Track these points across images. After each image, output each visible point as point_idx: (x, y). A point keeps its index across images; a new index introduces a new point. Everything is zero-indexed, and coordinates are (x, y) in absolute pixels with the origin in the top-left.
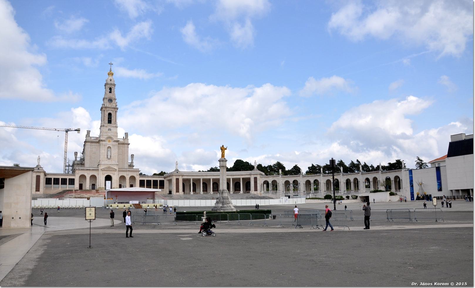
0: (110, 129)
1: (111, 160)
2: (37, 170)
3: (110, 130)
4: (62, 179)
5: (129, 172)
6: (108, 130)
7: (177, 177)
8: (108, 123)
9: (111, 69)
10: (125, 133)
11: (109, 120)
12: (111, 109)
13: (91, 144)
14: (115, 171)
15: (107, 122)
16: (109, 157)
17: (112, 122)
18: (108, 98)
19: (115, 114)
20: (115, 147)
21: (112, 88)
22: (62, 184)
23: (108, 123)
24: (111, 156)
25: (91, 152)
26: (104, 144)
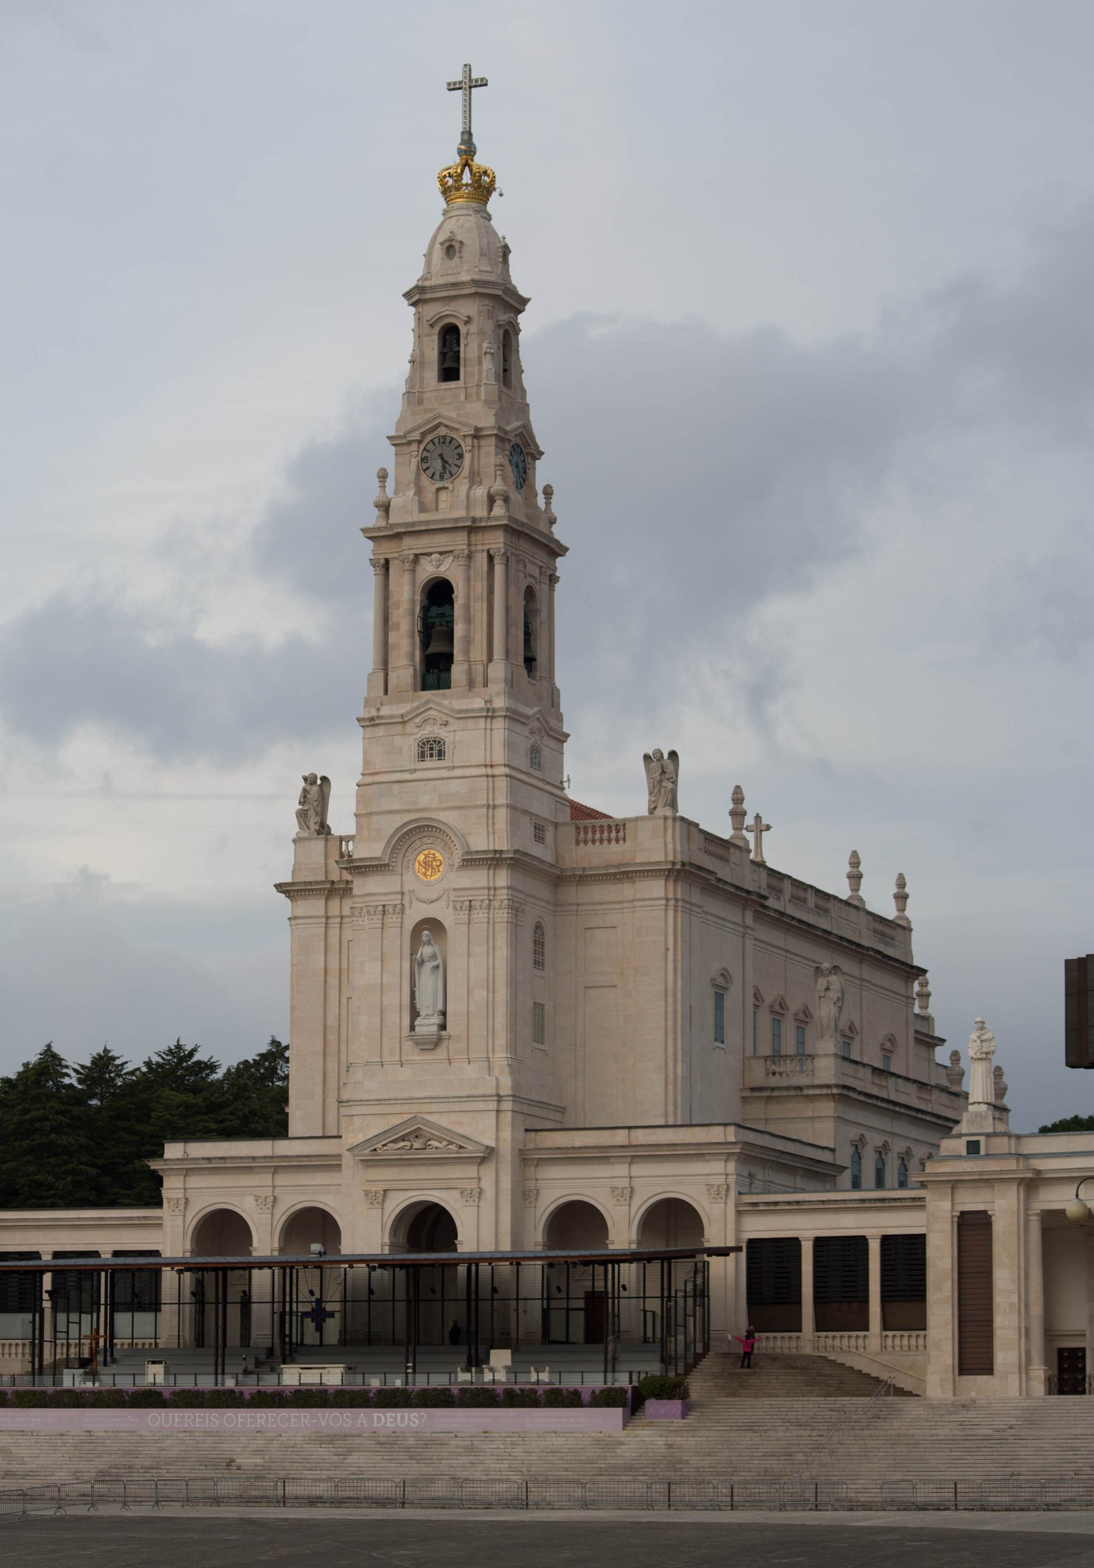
0: (438, 742)
1: (441, 1053)
3: (432, 749)
5: (633, 1159)
6: (415, 751)
7: (972, 1201)
9: (467, 137)
10: (647, 758)
11: (433, 649)
12: (442, 541)
13: (335, 903)
14: (483, 1160)
16: (427, 1025)
17: (458, 671)
18: (416, 436)
19: (479, 587)
20: (480, 916)
21: (463, 330)
24: (444, 1014)
25: (333, 981)
26: (380, 901)
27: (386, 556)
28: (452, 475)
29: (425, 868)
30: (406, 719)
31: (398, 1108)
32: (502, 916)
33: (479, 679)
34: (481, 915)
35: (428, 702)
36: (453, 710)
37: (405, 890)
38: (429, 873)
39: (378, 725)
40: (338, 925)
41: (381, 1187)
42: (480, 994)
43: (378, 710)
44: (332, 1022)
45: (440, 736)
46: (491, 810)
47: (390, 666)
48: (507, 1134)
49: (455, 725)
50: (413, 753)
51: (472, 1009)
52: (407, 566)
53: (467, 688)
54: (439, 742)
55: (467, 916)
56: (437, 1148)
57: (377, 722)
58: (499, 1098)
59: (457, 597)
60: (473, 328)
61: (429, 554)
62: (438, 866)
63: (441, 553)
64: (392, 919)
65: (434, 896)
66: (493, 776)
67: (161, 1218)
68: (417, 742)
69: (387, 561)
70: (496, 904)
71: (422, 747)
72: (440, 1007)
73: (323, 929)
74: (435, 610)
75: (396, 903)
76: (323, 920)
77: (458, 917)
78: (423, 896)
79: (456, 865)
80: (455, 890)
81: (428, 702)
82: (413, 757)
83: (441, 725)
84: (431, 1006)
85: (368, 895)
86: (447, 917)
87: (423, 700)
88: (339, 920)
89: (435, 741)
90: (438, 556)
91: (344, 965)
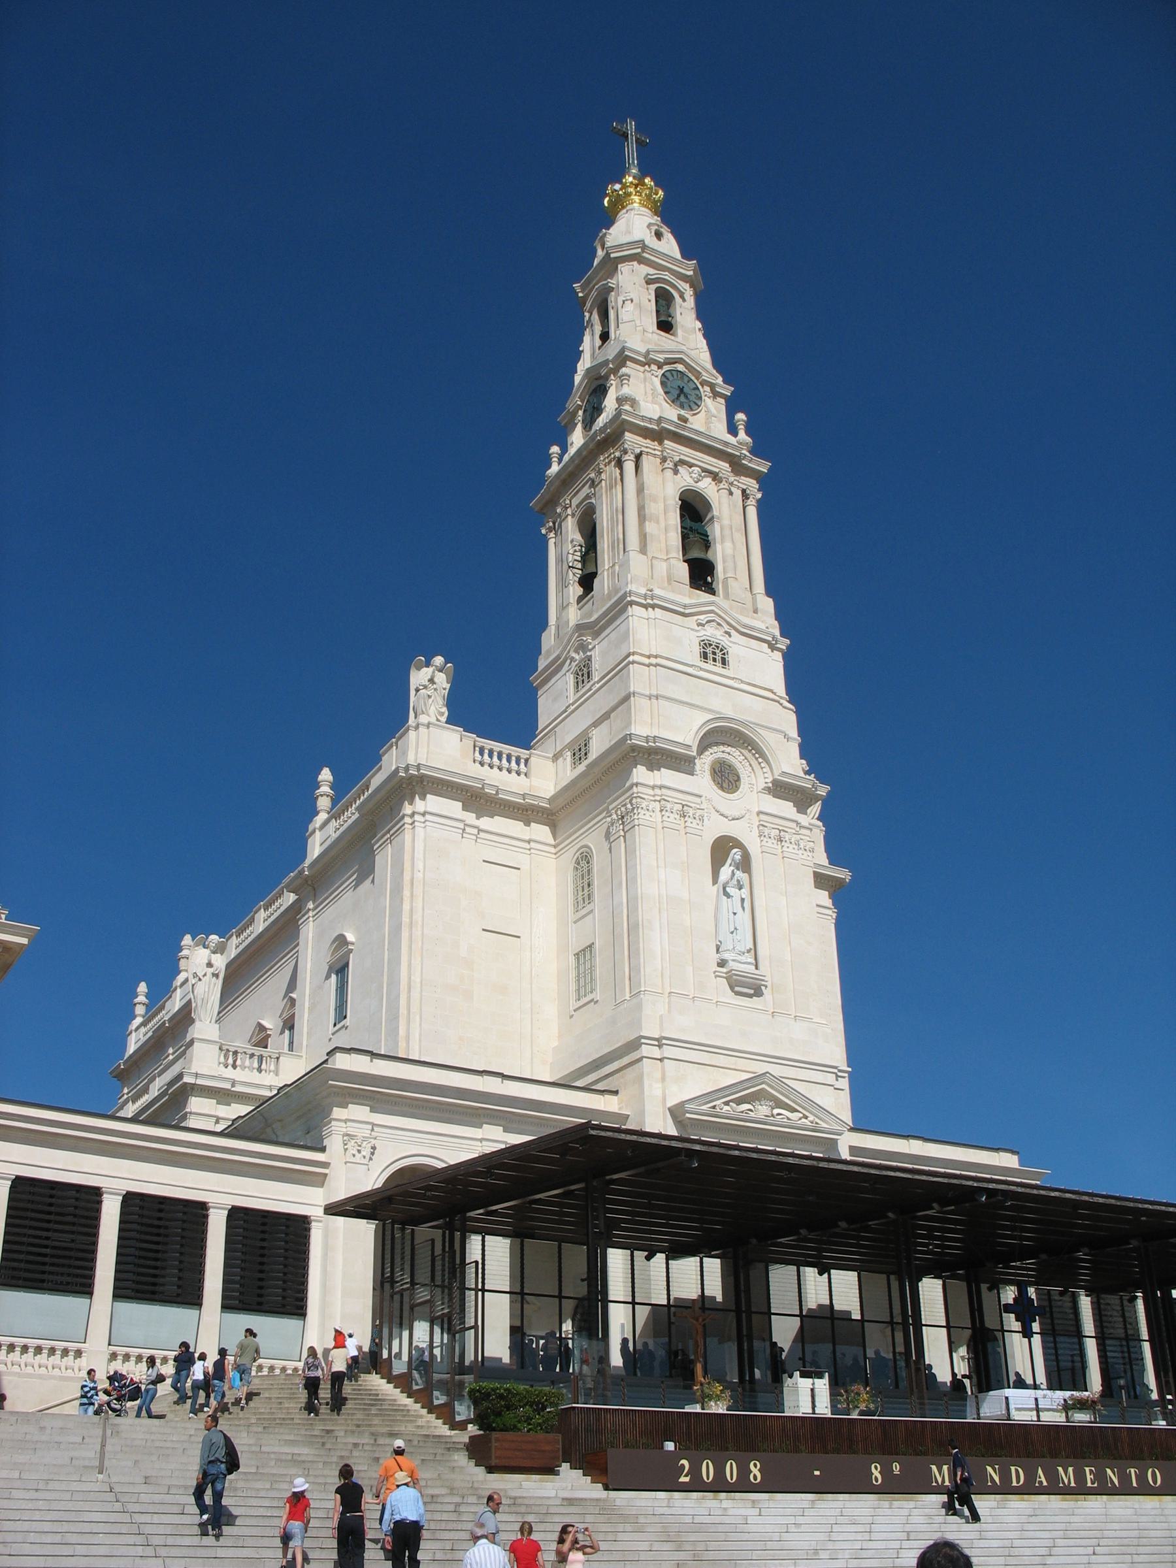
4: (132, 1201)
6: (697, 650)
11: (696, 554)
18: (661, 358)
27: (643, 449)
28: (692, 410)
30: (687, 611)
31: (721, 1060)
36: (738, 622)
38: (724, 785)
39: (653, 606)
45: (722, 643)
54: (722, 650)
56: (788, 1119)
57: (656, 601)
60: (685, 304)
61: (691, 465)
63: (704, 470)
65: (737, 814)
67: (325, 1165)
69: (641, 454)
71: (703, 648)
78: (722, 810)
80: (759, 813)
85: (661, 787)
90: (700, 470)
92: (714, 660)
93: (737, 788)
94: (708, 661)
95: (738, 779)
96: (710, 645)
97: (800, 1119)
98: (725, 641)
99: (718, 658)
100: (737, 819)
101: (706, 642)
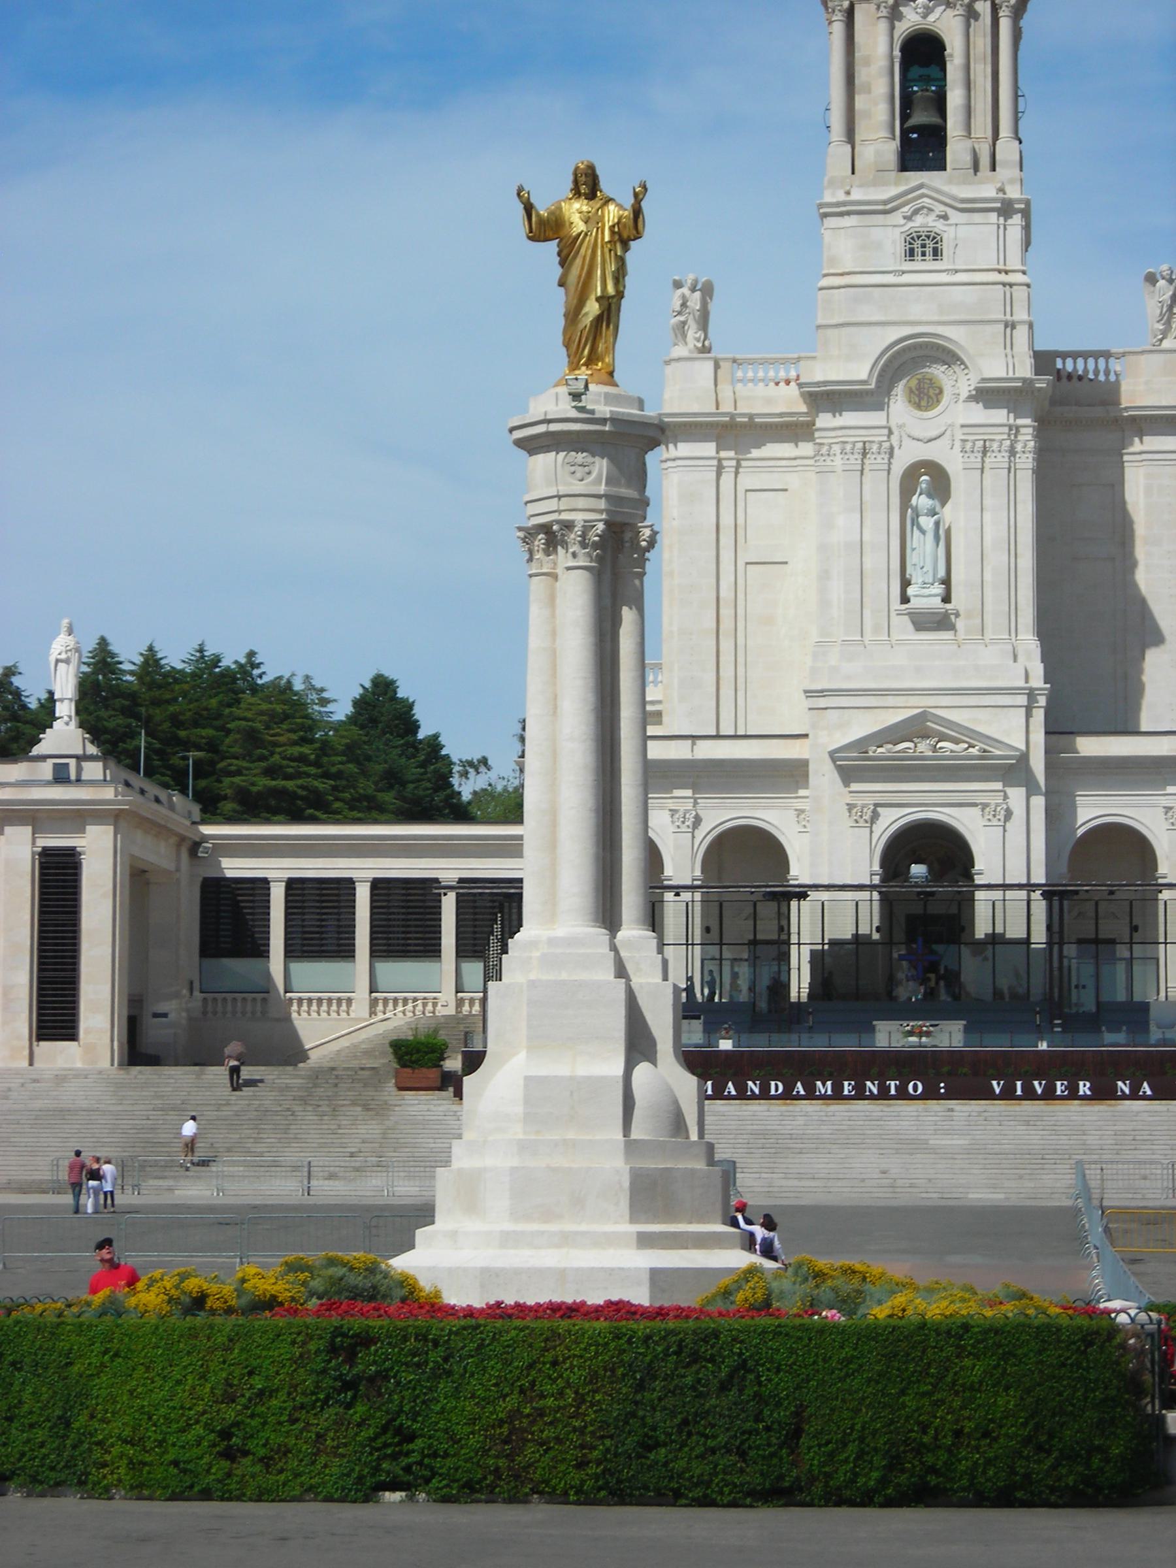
2: (48, 783)
6: (900, 248)
8: (905, 164)
11: (919, 118)
15: (890, 149)
16: (926, 597)
17: (956, 149)
19: (981, 43)
22: (383, 948)
23: (905, 164)
24: (947, 582)
29: (919, 396)
30: (889, 207)
31: (890, 701)
32: (1026, 462)
33: (985, 161)
34: (999, 459)
35: (921, 186)
36: (954, 198)
37: (893, 424)
40: (733, 469)
41: (870, 800)
42: (997, 559)
43: (848, 193)
44: (726, 593)
45: (936, 230)
46: (1008, 330)
47: (858, 138)
48: (1038, 737)
49: (955, 217)
50: (898, 252)
51: (988, 577)
52: (884, 12)
53: (972, 171)
54: (934, 238)
55: (979, 459)
58: (1031, 694)
59: (951, 55)
62: (937, 395)
64: (876, 461)
65: (934, 434)
66: (1011, 285)
68: (904, 235)
70: (1019, 447)
72: (942, 573)
73: (714, 474)
74: (916, 71)
75: (881, 439)
76: (715, 462)
77: (967, 460)
78: (916, 434)
79: (964, 394)
80: (963, 426)
81: (921, 186)
82: (898, 255)
83: (940, 217)
84: (931, 574)
86: (953, 463)
87: (913, 184)
88: (734, 463)
89: (928, 237)
91: (741, 521)
92: (924, 254)
93: (928, 408)
94: (916, 258)
95: (941, 392)
96: (919, 237)
97: (967, 749)
98: (939, 226)
99: (929, 250)
100: (935, 439)
101: (914, 234)
